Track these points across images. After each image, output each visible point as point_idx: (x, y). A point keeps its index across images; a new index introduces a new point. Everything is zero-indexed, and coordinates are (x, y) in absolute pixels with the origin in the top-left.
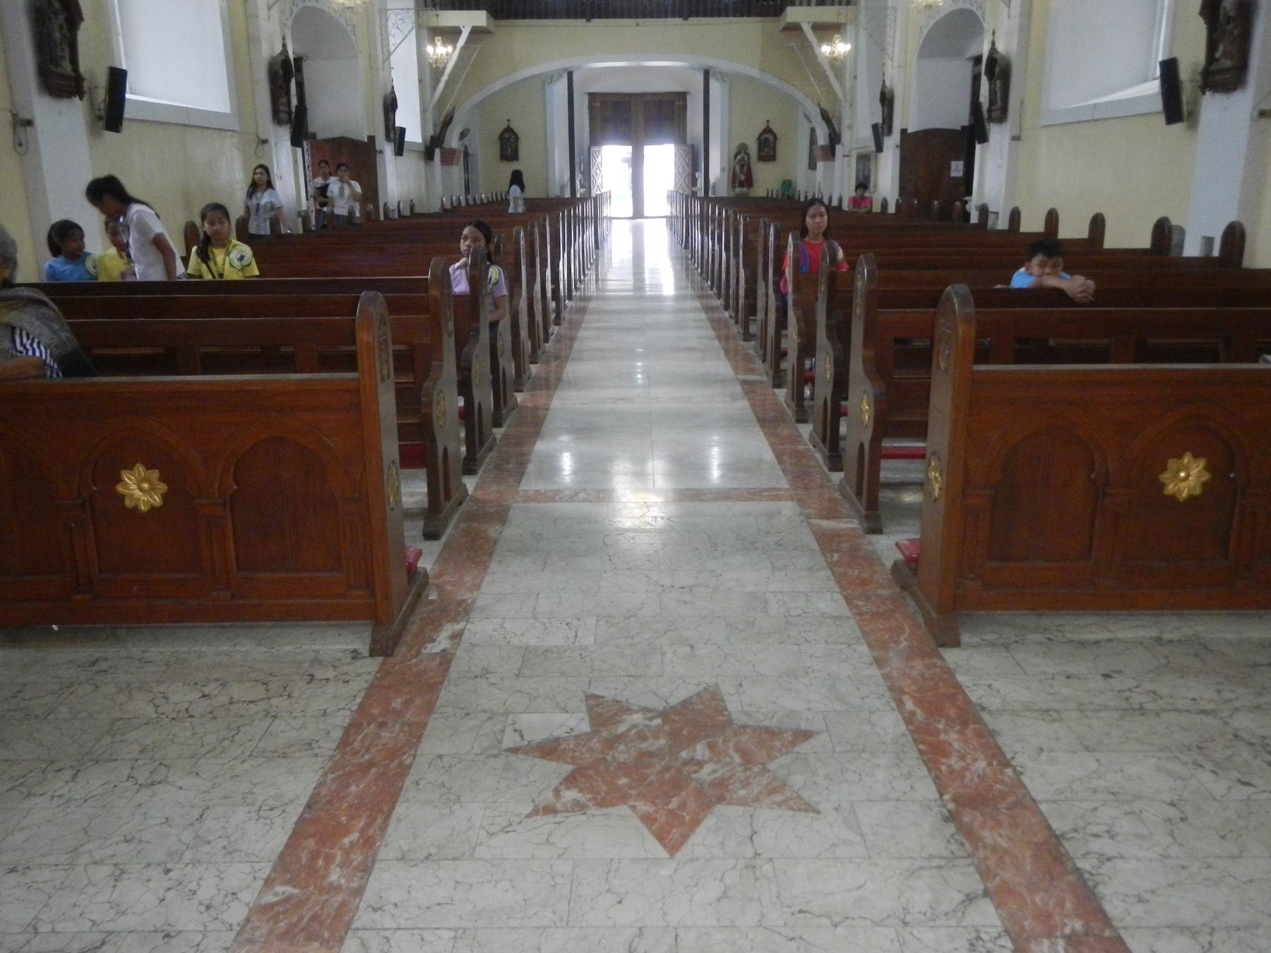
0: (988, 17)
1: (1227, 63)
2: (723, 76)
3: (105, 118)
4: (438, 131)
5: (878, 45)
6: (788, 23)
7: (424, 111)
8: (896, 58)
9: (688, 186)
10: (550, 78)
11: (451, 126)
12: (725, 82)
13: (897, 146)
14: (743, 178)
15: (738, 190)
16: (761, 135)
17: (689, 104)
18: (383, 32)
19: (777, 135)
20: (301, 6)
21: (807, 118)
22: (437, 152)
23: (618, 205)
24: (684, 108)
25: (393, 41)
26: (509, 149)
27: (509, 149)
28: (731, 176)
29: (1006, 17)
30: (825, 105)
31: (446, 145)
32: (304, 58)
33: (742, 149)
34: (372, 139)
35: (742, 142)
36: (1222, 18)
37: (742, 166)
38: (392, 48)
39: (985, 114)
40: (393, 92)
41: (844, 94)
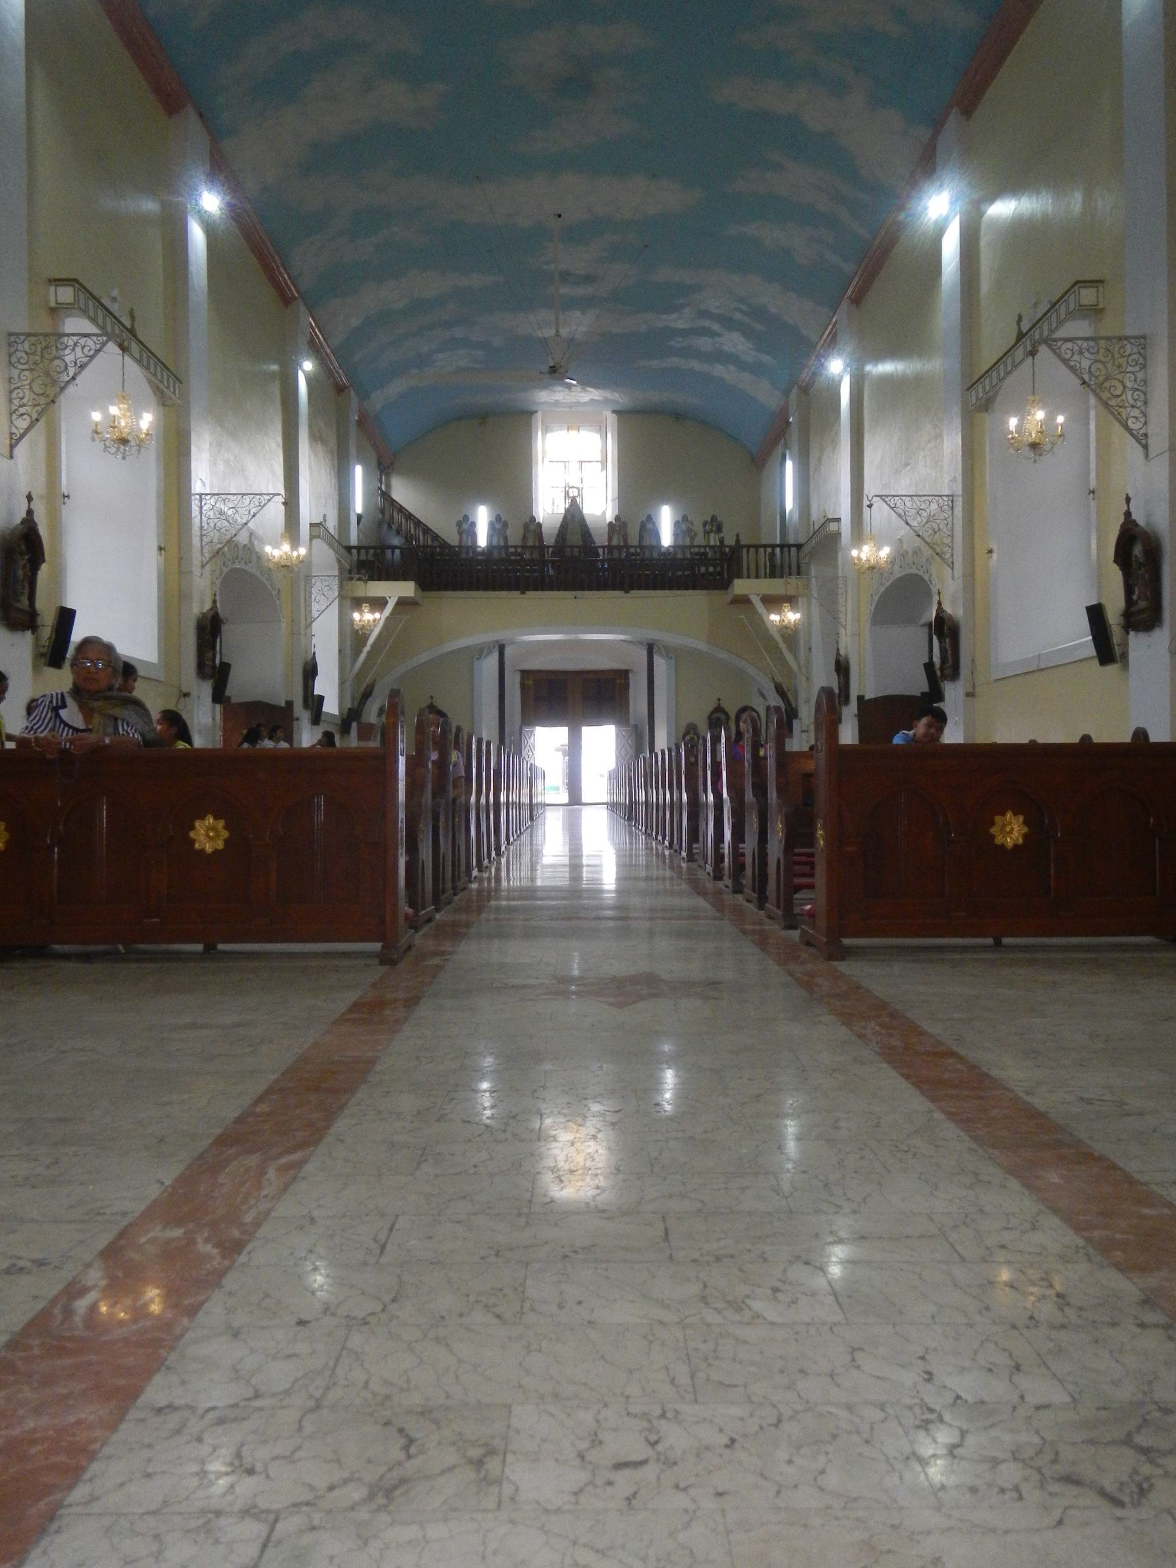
0: (935, 580)
1: (1143, 604)
2: (670, 652)
3: (48, 655)
4: (356, 703)
5: (832, 616)
6: (737, 595)
7: (342, 682)
8: (848, 627)
10: (480, 652)
11: (370, 699)
12: (671, 658)
13: (856, 716)
16: (713, 712)
18: (308, 598)
20: (231, 566)
22: (354, 725)
23: (553, 790)
24: (626, 687)
25: (315, 607)
29: (950, 577)
30: (779, 679)
31: (364, 719)
33: (691, 729)
34: (290, 704)
36: (1134, 566)
38: (315, 614)
39: (939, 673)
40: (314, 658)
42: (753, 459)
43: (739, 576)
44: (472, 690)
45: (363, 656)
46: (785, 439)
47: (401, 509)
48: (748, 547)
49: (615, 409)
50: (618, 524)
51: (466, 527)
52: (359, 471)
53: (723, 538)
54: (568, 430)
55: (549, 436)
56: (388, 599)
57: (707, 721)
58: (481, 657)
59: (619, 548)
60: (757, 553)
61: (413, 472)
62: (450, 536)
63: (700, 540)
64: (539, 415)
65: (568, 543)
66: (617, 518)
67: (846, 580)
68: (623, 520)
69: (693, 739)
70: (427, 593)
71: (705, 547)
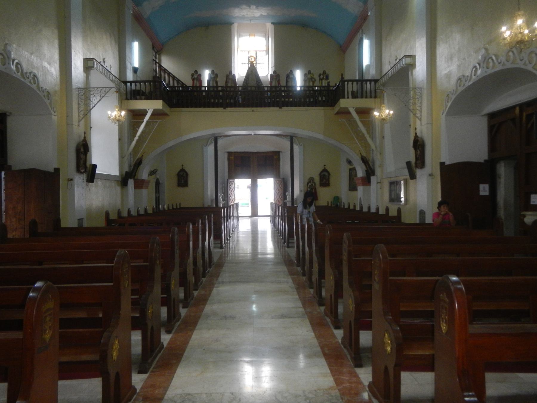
6: (341, 108)
7: (122, 157)
9: (282, 200)
10: (203, 141)
12: (301, 145)
19: (330, 172)
21: (349, 162)
22: (131, 182)
23: (244, 210)
24: (279, 159)
26: (183, 180)
27: (183, 180)
30: (364, 154)
32: (8, 114)
33: (311, 180)
35: (311, 176)
41: (376, 147)
42: (341, 47)
43: (344, 97)
44: (203, 161)
45: (134, 143)
47: (165, 70)
48: (348, 81)
49: (272, 21)
50: (275, 75)
51: (197, 77)
52: (136, 46)
53: (329, 82)
54: (250, 36)
55: (241, 39)
56: (147, 110)
58: (207, 145)
59: (276, 87)
60: (352, 84)
61: (174, 54)
62: (188, 82)
64: (236, 25)
65: (249, 85)
67: (421, 91)
68: (277, 73)
71: (320, 87)
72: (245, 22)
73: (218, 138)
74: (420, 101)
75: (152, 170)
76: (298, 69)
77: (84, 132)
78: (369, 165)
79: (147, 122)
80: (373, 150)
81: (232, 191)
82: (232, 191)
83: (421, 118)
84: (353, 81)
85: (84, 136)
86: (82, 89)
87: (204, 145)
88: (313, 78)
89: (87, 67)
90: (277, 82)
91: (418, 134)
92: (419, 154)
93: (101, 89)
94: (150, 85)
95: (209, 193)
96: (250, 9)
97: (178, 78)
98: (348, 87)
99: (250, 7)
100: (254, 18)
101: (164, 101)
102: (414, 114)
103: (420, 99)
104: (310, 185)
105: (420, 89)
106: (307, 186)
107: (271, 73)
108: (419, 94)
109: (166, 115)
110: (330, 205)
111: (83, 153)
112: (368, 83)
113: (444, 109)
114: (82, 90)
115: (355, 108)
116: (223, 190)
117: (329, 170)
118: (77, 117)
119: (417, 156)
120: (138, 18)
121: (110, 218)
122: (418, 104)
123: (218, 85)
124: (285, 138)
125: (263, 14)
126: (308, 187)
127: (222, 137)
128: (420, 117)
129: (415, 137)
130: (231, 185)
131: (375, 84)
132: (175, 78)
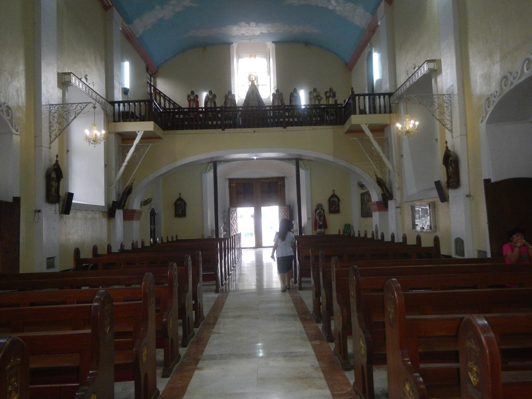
6: (352, 125)
12: (308, 169)
14: (321, 223)
15: (318, 230)
17: (286, 182)
21: (362, 186)
27: (180, 210)
28: (314, 222)
30: (380, 176)
33: (319, 207)
37: (320, 217)
41: (393, 167)
42: (347, 64)
43: (355, 113)
46: (371, 43)
48: (359, 95)
49: (274, 40)
50: (278, 94)
51: (194, 98)
52: (127, 66)
53: (337, 100)
55: (240, 60)
56: (137, 132)
57: (328, 202)
58: (206, 172)
61: (169, 76)
62: (183, 103)
63: (324, 102)
64: (235, 46)
65: (250, 105)
66: (277, 91)
67: (450, 97)
68: (280, 92)
69: (321, 212)
70: (166, 132)
72: (245, 41)
73: (218, 164)
74: (449, 110)
75: (146, 199)
76: (302, 89)
77: (56, 155)
78: (386, 188)
79: (137, 146)
80: (389, 170)
81: (234, 221)
82: (234, 220)
83: (452, 129)
84: (364, 95)
85: (57, 159)
86: (55, 106)
87: (203, 171)
88: (319, 96)
89: (64, 82)
90: (280, 101)
91: (449, 148)
92: (452, 171)
93: (76, 105)
94: (140, 105)
95: (209, 224)
96: (250, 26)
97: (174, 101)
98: (359, 102)
99: (249, 24)
100: (254, 37)
101: (156, 122)
102: (443, 125)
103: (449, 107)
104: (318, 213)
105: (449, 96)
106: (316, 213)
107: (273, 92)
108: (449, 102)
109: (159, 138)
110: (341, 234)
111: (55, 179)
112: (382, 97)
113: (484, 116)
114: (55, 107)
115: (368, 125)
116: (224, 219)
117: (338, 196)
118: (48, 137)
119: (450, 174)
120: (128, 37)
121: (81, 257)
122: (448, 114)
123: (216, 105)
124: (290, 162)
125: (263, 32)
126: (316, 214)
127: (222, 163)
128: (451, 129)
129: (445, 151)
130: (233, 214)
131: (389, 98)
132: (171, 101)
